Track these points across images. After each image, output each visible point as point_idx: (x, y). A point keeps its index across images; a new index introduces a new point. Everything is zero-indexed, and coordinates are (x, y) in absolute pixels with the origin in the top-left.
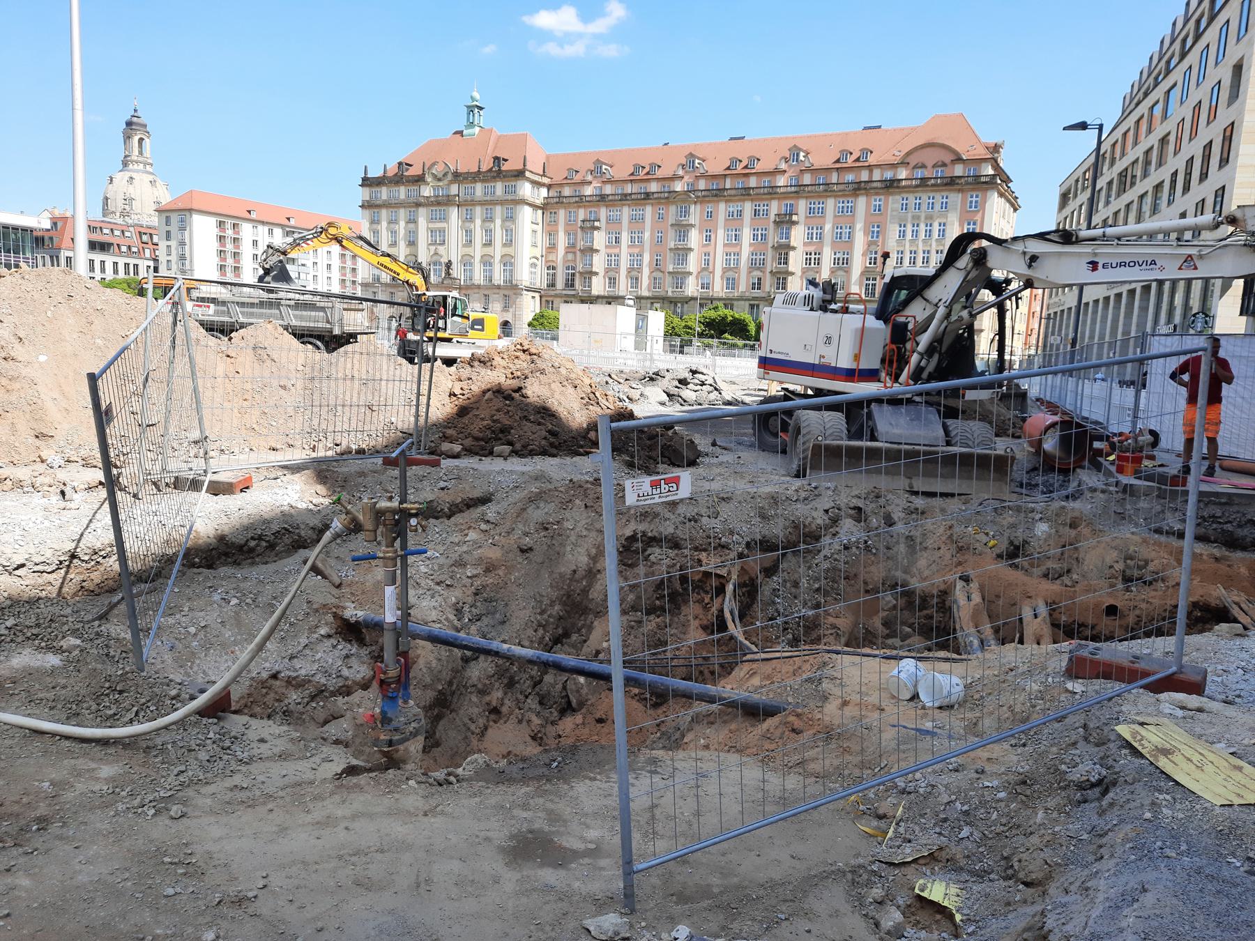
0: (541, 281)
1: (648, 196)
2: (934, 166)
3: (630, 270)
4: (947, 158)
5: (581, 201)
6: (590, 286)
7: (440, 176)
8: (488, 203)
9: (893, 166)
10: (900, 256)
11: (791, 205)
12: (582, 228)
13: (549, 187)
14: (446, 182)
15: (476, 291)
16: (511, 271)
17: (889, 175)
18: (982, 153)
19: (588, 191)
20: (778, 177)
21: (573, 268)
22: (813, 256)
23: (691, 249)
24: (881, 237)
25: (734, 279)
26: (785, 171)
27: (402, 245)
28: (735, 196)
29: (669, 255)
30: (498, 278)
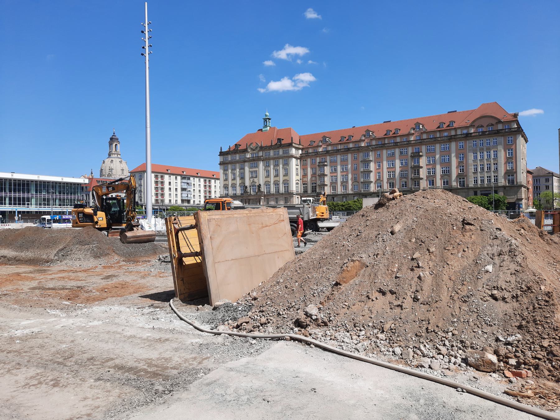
2: (487, 126)
3: (342, 183)
5: (317, 154)
7: (254, 148)
8: (276, 159)
9: (467, 127)
10: (475, 167)
12: (318, 166)
13: (302, 149)
14: (257, 151)
16: (287, 187)
17: (465, 131)
18: (511, 118)
19: (320, 150)
20: (410, 137)
21: (315, 184)
23: (371, 171)
24: (465, 159)
25: (393, 183)
26: (414, 134)
27: (238, 179)
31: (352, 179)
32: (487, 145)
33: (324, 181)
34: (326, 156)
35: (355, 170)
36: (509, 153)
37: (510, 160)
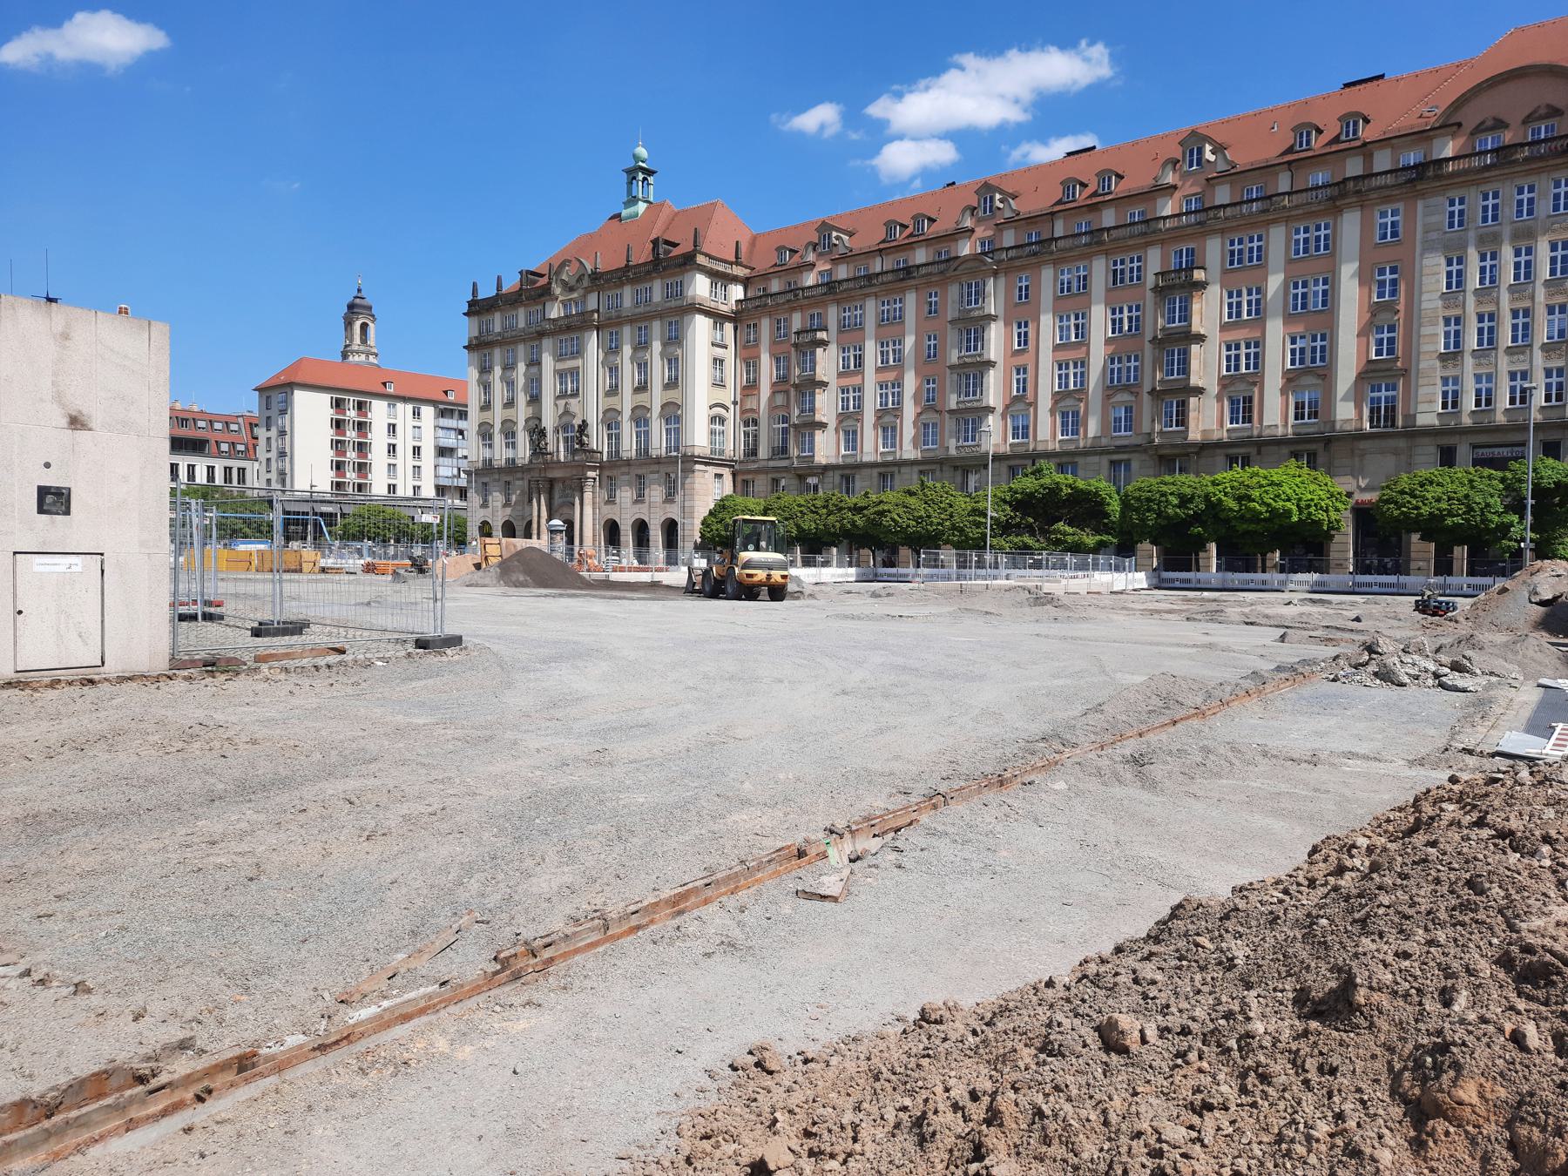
0: (732, 445)
1: (907, 273)
2: (1524, 122)
3: (881, 414)
5: (795, 297)
6: (812, 449)
7: (573, 282)
8: (640, 320)
9: (1422, 136)
12: (796, 345)
13: (746, 282)
15: (625, 469)
16: (677, 430)
17: (1412, 157)
20: (1160, 201)
22: (1243, 351)
23: (990, 364)
24: (1402, 287)
25: (1076, 414)
26: (1175, 187)
27: (522, 399)
28: (1071, 249)
29: (950, 379)
30: (659, 443)
31: (916, 397)
32: (1520, 213)
33: (813, 410)
34: (824, 304)
35: (930, 357)
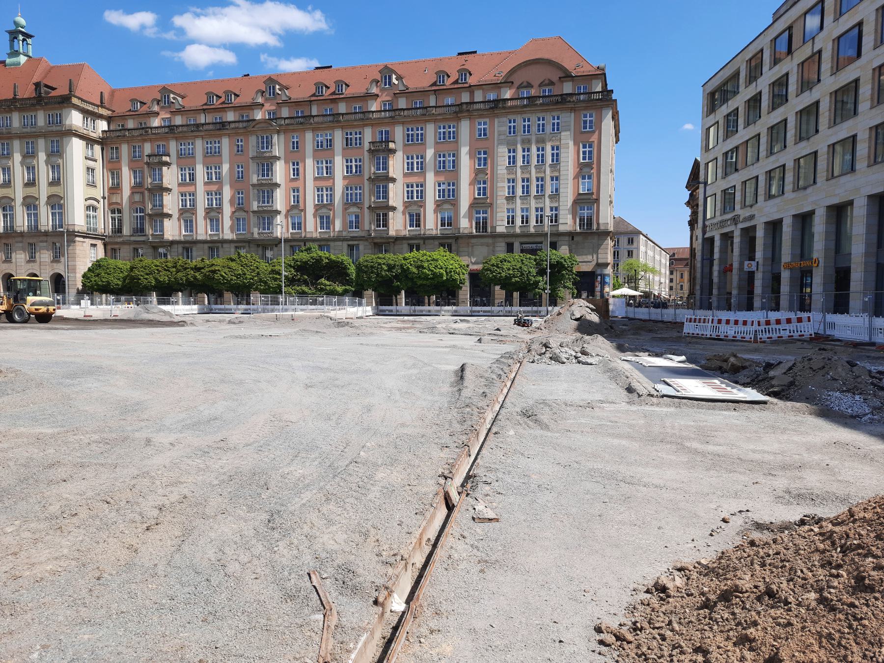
1: (222, 126)
2: (540, 86)
3: (209, 211)
4: (555, 76)
5: (145, 133)
6: (162, 230)
8: (29, 137)
9: (496, 86)
11: (387, 132)
12: (148, 164)
13: (109, 120)
15: (20, 239)
16: (61, 214)
17: (492, 96)
19: (156, 122)
20: (370, 102)
21: (142, 211)
22: (415, 189)
23: (277, 185)
24: (489, 161)
26: (377, 96)
28: (322, 123)
29: (253, 192)
30: (46, 221)
31: (232, 202)
32: (539, 130)
33: (162, 206)
34: (167, 139)
35: (239, 179)
36: (584, 153)
37: (586, 170)
